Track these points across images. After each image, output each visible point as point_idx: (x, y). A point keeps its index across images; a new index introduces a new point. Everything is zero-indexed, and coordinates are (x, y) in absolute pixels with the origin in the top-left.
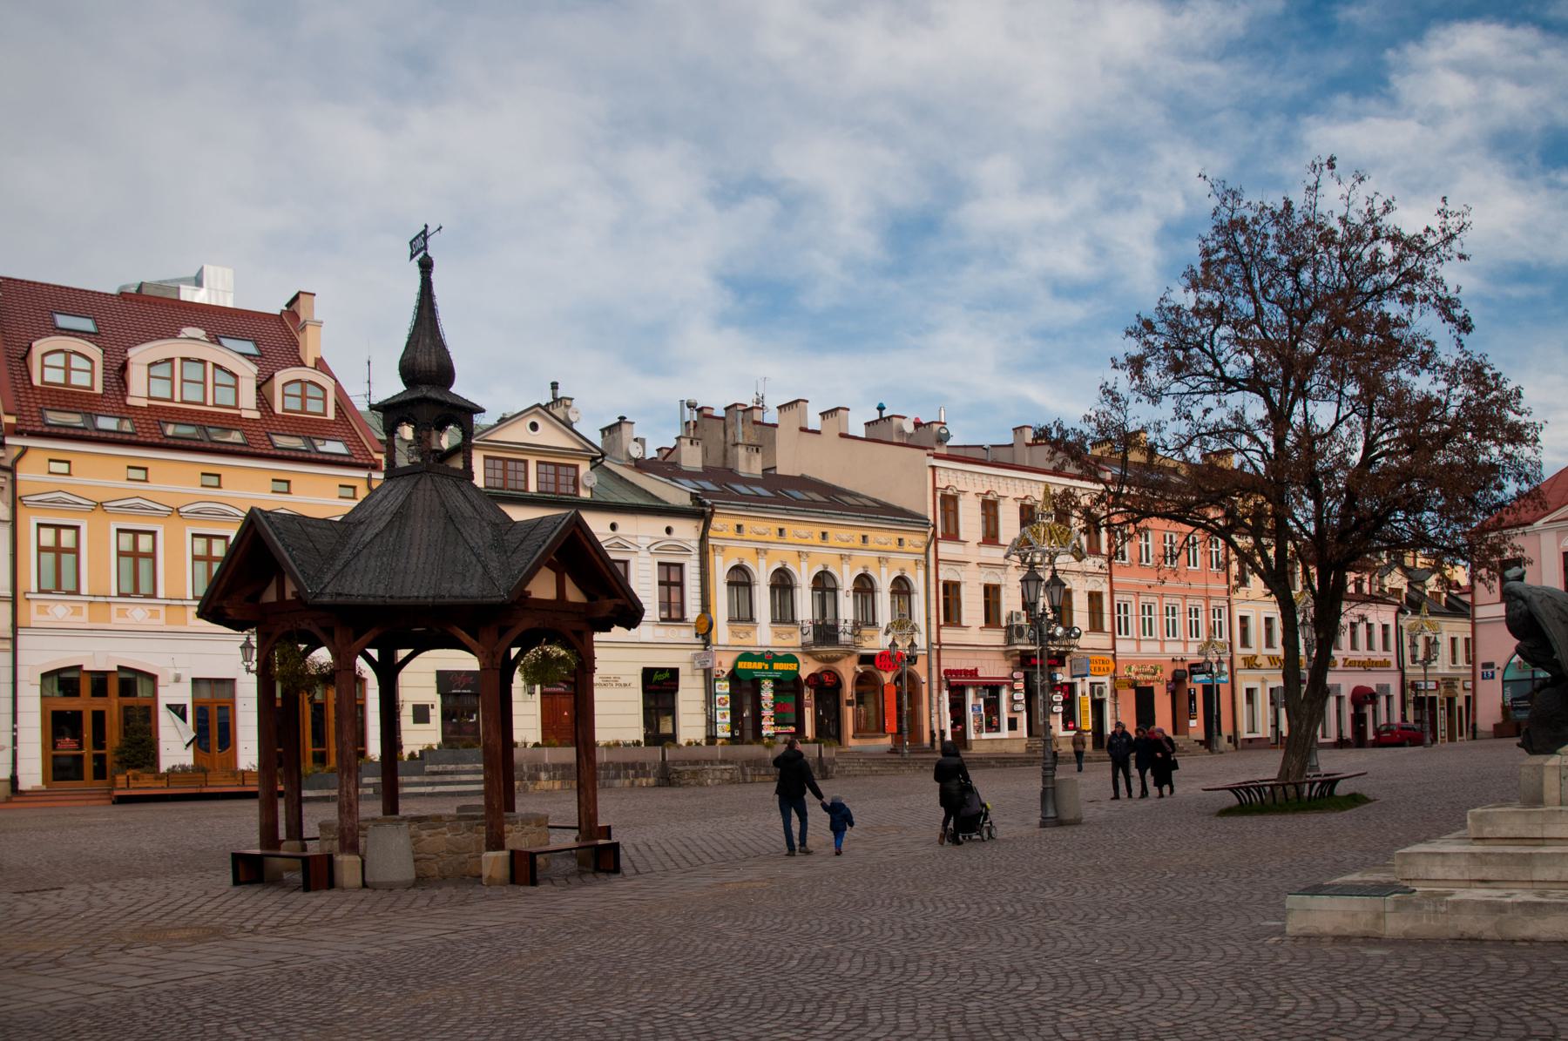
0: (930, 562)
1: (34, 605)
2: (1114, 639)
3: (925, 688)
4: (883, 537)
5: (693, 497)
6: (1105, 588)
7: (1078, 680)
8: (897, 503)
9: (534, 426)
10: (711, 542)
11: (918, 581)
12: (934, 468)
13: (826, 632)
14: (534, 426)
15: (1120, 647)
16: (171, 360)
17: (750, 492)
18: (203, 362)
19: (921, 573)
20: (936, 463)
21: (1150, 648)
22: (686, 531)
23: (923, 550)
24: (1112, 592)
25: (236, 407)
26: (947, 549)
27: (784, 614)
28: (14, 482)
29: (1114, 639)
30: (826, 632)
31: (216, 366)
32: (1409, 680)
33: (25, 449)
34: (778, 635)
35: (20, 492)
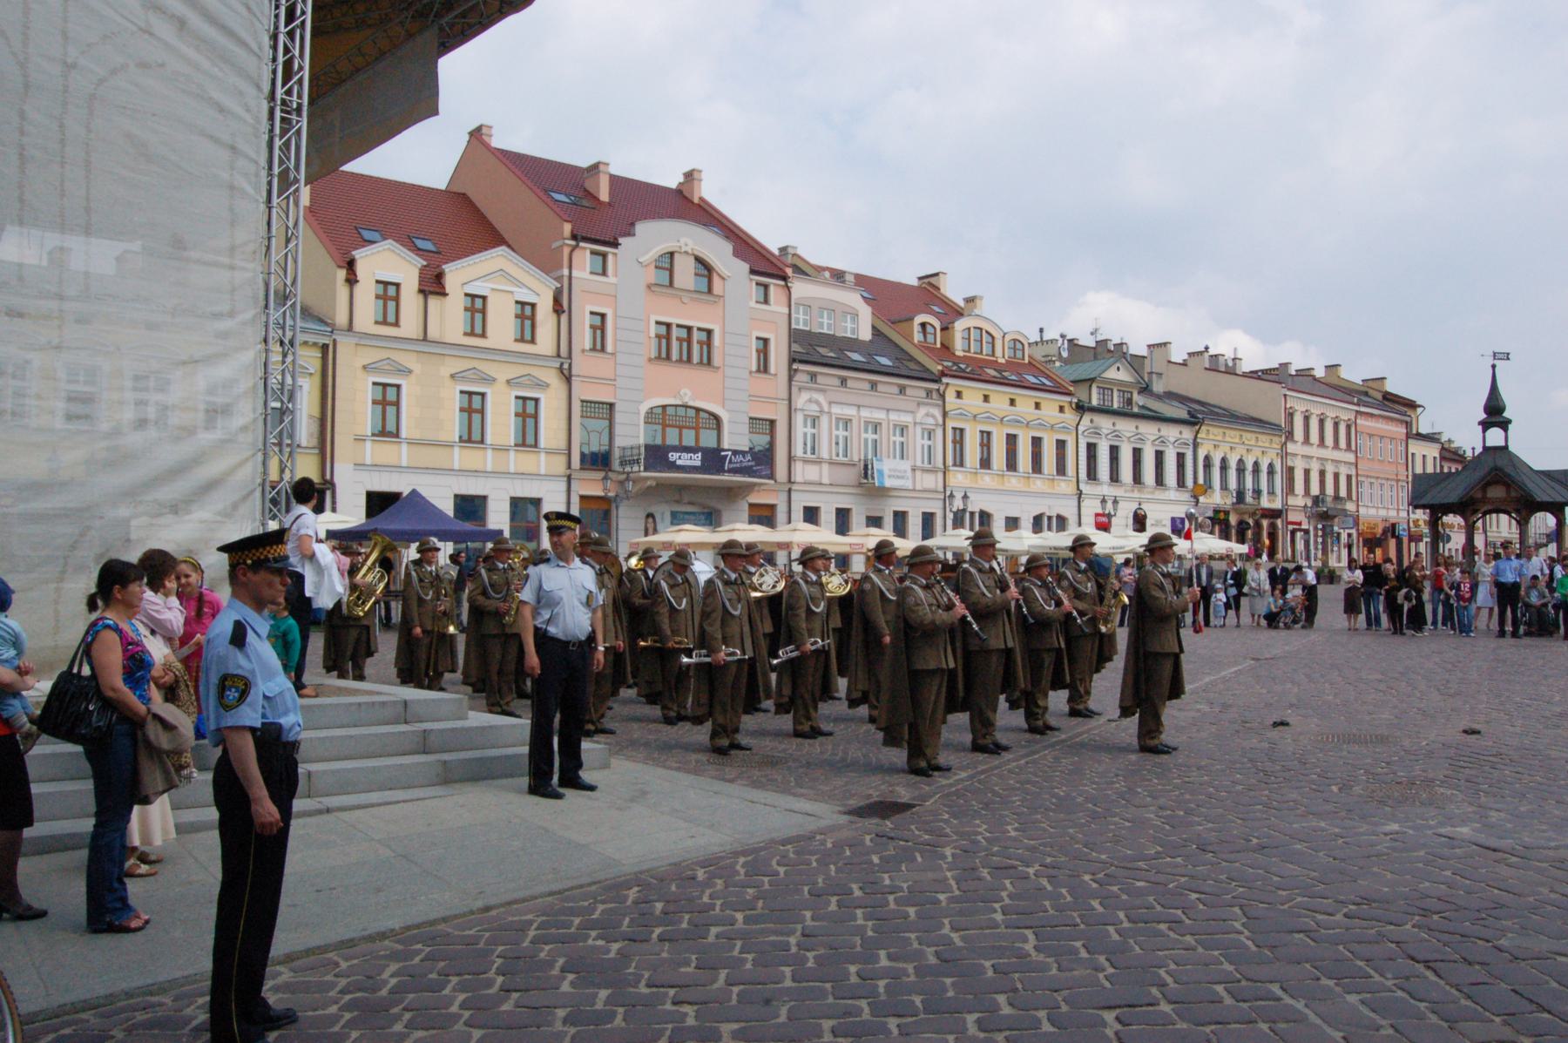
0: (1284, 455)
1: (951, 473)
2: (1358, 506)
3: (1280, 532)
4: (1264, 440)
5: (1189, 413)
6: (1353, 472)
7: (1342, 531)
8: (1264, 418)
9: (1118, 369)
10: (1198, 440)
11: (1278, 467)
12: (1285, 395)
13: (1240, 495)
14: (1118, 369)
15: (1362, 511)
16: (969, 329)
17: (1038, 382)
18: (981, 329)
19: (1279, 460)
20: (1288, 393)
21: (1372, 512)
22: (1187, 433)
23: (1279, 447)
24: (1357, 475)
25: (993, 355)
26: (1291, 447)
27: (1224, 487)
28: (944, 402)
29: (1358, 506)
30: (1240, 495)
31: (987, 332)
32: (1489, 539)
33: (947, 384)
34: (1222, 497)
35: (947, 409)
